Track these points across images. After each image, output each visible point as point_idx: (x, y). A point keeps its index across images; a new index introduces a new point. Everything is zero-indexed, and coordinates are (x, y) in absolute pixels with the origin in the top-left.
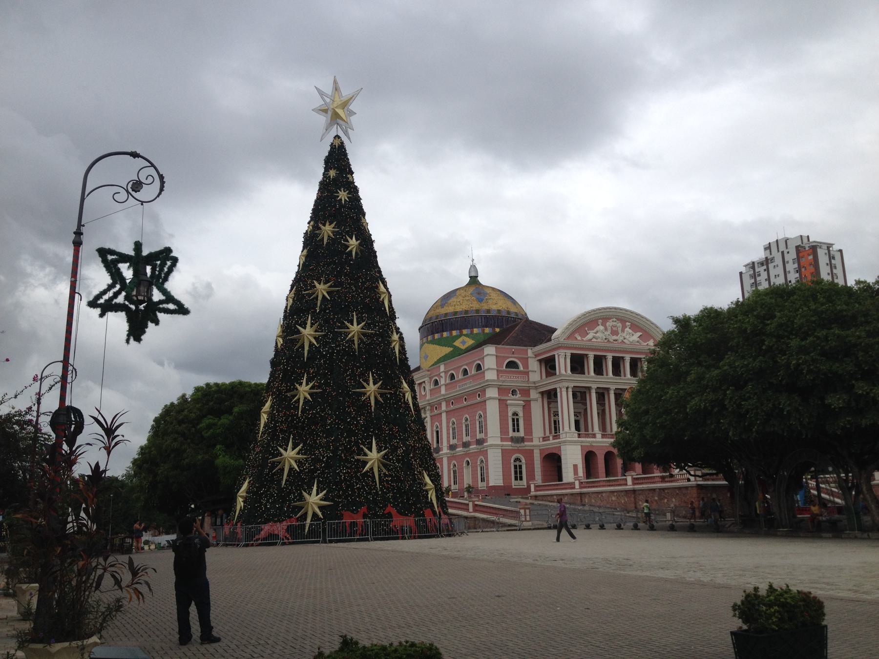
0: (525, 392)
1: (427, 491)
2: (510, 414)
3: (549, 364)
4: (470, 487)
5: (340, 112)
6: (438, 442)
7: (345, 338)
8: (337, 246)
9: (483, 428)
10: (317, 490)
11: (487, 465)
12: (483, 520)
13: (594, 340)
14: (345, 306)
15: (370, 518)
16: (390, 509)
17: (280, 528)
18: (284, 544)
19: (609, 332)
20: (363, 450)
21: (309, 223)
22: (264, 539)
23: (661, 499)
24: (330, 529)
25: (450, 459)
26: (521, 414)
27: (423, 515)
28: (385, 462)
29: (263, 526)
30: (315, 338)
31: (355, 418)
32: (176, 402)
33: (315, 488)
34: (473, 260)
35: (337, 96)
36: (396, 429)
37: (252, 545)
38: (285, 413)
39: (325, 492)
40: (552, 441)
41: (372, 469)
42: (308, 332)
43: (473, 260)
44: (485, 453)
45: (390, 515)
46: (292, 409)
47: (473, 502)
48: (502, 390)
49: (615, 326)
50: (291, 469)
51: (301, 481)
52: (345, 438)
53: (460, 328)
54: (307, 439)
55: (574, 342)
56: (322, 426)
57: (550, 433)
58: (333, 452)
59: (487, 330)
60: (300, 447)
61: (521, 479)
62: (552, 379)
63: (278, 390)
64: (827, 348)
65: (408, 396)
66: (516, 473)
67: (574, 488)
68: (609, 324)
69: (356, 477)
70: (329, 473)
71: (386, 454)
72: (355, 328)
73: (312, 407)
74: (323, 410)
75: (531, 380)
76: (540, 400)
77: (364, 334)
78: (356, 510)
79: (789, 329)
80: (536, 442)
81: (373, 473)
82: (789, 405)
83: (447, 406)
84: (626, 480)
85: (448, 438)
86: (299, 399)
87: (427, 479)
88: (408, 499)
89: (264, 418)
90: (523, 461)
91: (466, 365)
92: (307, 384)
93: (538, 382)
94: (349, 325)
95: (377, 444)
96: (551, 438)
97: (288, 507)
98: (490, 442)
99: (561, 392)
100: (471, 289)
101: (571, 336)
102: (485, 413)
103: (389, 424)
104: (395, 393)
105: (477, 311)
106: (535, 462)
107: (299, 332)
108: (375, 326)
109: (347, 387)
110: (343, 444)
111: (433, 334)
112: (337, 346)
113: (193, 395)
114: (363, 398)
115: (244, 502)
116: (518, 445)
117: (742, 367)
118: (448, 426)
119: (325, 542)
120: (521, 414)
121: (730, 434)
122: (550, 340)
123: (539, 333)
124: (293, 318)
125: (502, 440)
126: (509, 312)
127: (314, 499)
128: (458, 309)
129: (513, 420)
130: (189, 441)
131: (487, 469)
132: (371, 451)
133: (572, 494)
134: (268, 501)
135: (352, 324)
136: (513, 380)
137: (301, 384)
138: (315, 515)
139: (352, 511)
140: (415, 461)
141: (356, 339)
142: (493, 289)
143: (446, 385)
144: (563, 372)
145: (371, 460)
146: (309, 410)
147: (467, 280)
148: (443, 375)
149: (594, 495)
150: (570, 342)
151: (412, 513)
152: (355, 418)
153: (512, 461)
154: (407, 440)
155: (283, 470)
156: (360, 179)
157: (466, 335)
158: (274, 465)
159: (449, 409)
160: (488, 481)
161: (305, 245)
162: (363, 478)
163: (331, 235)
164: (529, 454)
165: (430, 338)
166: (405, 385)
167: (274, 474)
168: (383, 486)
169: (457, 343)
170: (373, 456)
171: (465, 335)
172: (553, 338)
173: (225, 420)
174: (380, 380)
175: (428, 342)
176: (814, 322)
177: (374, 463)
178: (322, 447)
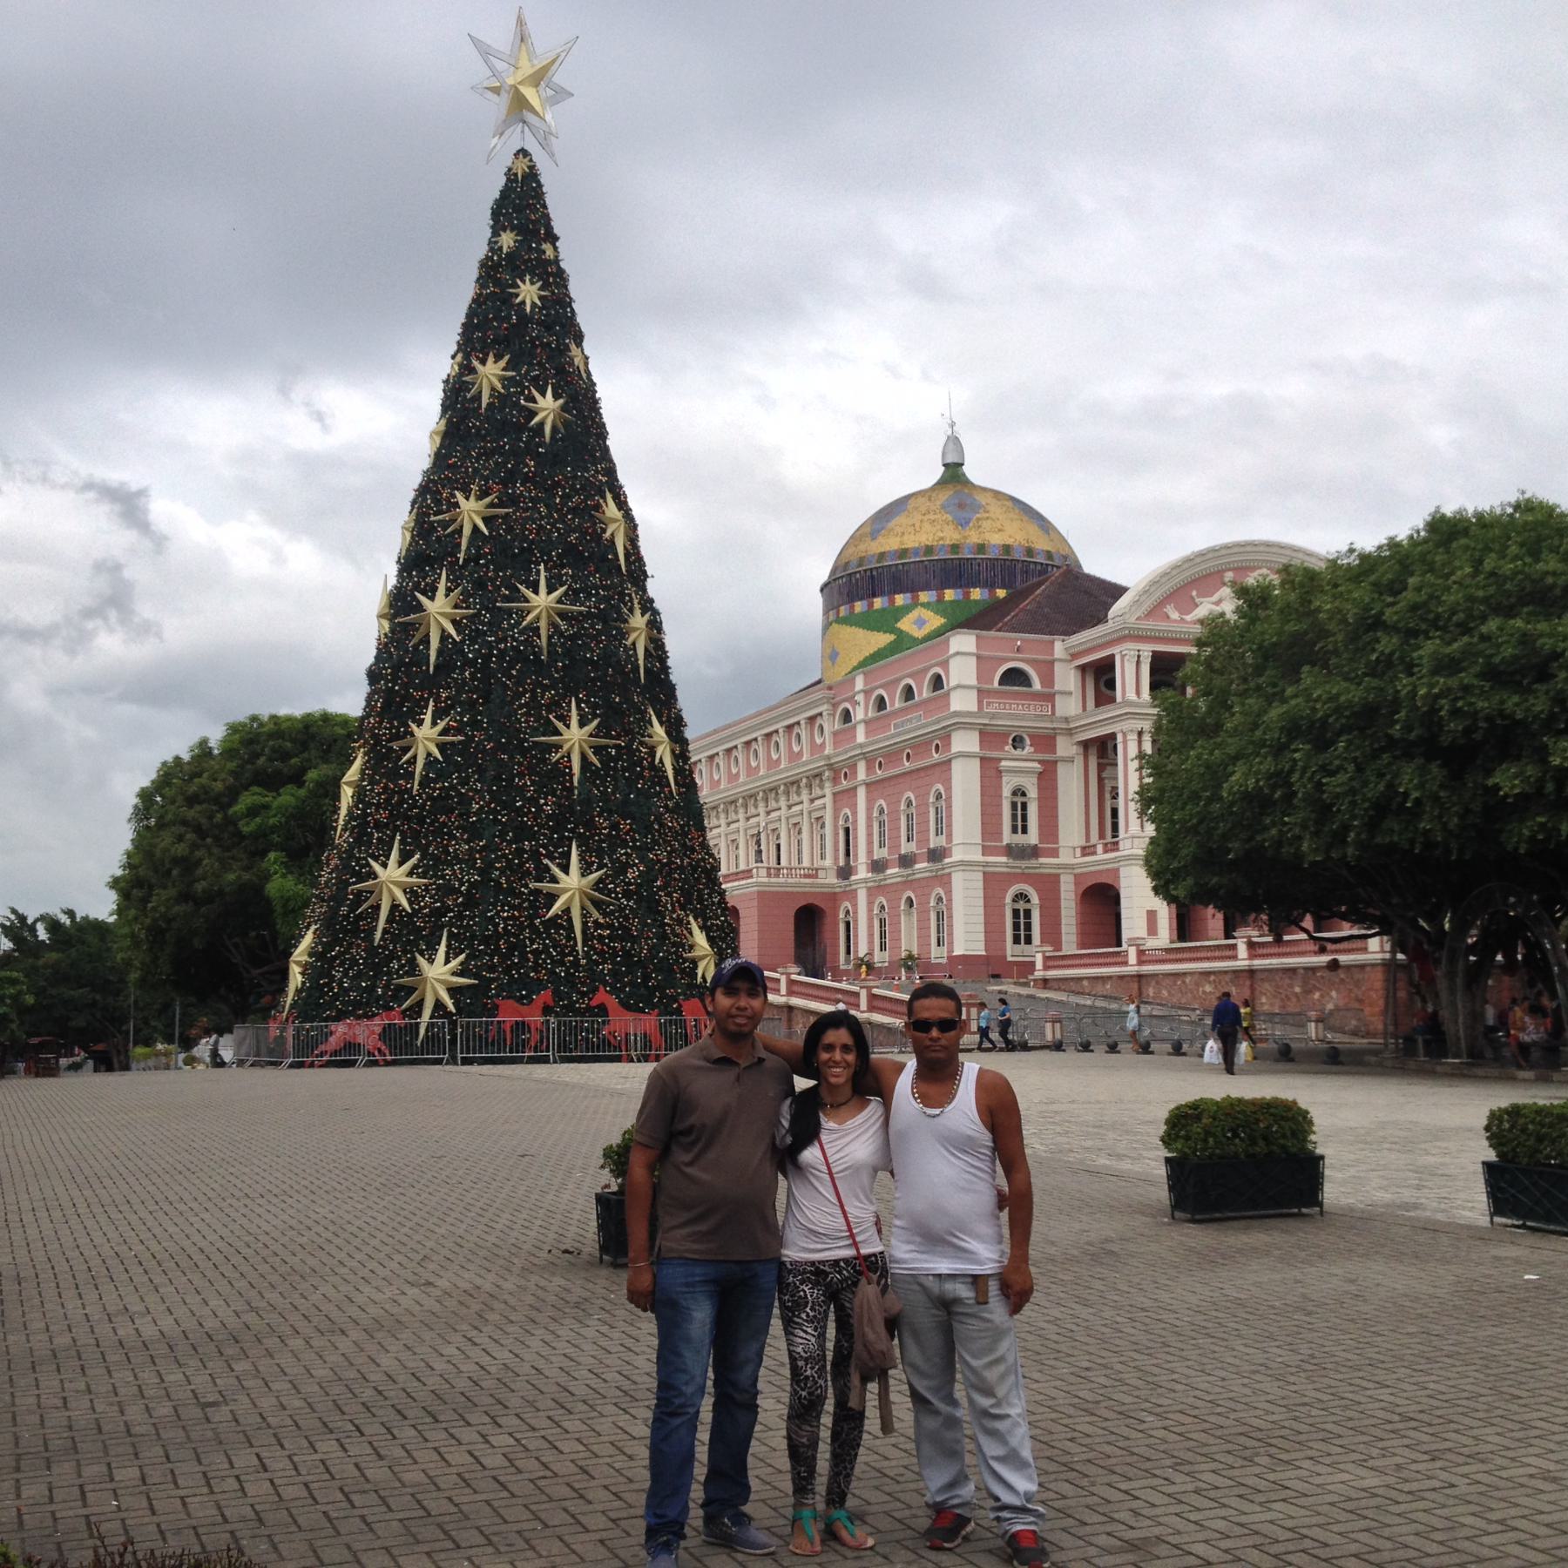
0: (1045, 742)
1: (694, 962)
2: (1006, 792)
3: (1101, 675)
4: (910, 957)
5: (529, 93)
6: (848, 853)
7: (518, 623)
8: (508, 416)
9: (944, 825)
10: (447, 953)
11: (950, 909)
12: (881, 1026)
14: (522, 549)
15: (557, 1015)
16: (603, 996)
17: (366, 1031)
18: (374, 1063)
20: (548, 869)
21: (453, 357)
22: (335, 1053)
23: (1308, 991)
24: (472, 1034)
25: (872, 892)
26: (1033, 793)
27: (679, 1012)
28: (597, 899)
29: (333, 1026)
30: (454, 622)
31: (533, 801)
32: (186, 757)
33: (442, 949)
34: (952, 425)
35: (524, 55)
36: (625, 825)
37: (312, 1065)
38: (385, 788)
39: (462, 957)
40: (1101, 855)
41: (567, 911)
42: (439, 608)
43: (952, 425)
44: (945, 881)
45: (603, 1010)
46: (401, 777)
47: (869, 988)
48: (988, 737)
50: (395, 907)
51: (414, 933)
52: (510, 843)
53: (913, 589)
54: (429, 844)
55: (1162, 625)
56: (461, 815)
57: (1102, 836)
58: (481, 872)
59: (977, 594)
60: (414, 860)
61: (1028, 941)
62: (1108, 712)
63: (374, 736)
64: (1497, 660)
65: (664, 753)
66: (1016, 926)
67: (1126, 963)
69: (532, 926)
70: (472, 918)
71: (600, 880)
72: (542, 601)
73: (442, 775)
74: (464, 782)
75: (1058, 713)
76: (1079, 761)
77: (562, 615)
78: (528, 996)
79: (1431, 616)
80: (1065, 858)
81: (570, 920)
82: (1421, 786)
83: (869, 769)
84: (1234, 947)
85: (870, 843)
86: (415, 757)
87: (700, 938)
88: (646, 978)
89: (347, 793)
90: (1035, 900)
91: (909, 676)
92: (434, 724)
93: (1078, 718)
94: (529, 593)
95: (582, 858)
96: (1100, 848)
97: (386, 987)
98: (957, 855)
99: (1125, 742)
100: (944, 496)
101: (1156, 611)
102: (949, 789)
103: (610, 812)
104: (629, 746)
105: (955, 548)
106: (1063, 904)
107: (420, 608)
108: (589, 596)
109: (519, 731)
110: (505, 856)
111: (851, 598)
112: (499, 641)
113: (224, 741)
114: (555, 757)
115: (303, 974)
116: (1024, 864)
117: (1330, 699)
118: (869, 818)
119: (455, 1063)
120: (1033, 793)
121: (1305, 846)
122: (1101, 619)
123: (1085, 599)
124: (410, 576)
125: (986, 851)
126: (1030, 552)
127: (439, 972)
128: (911, 542)
129: (1014, 805)
130: (209, 840)
131: (950, 917)
132: (566, 872)
133: (1121, 977)
134: (345, 974)
135: (536, 592)
136: (1016, 713)
137: (420, 723)
138: (439, 1005)
139: (520, 999)
140: (669, 895)
141: (543, 624)
142: (997, 494)
143: (867, 722)
144: (1131, 696)
145: (565, 890)
146: (435, 781)
147: (940, 471)
148: (860, 698)
149: (1168, 981)
150: (1150, 624)
151: (653, 1007)
152: (533, 801)
153: (1008, 899)
154: (651, 850)
155: (377, 908)
156: (572, 254)
157: (926, 605)
158: (360, 897)
159: (873, 778)
160: (951, 943)
161: (445, 408)
162: (547, 931)
163: (499, 386)
164: (1049, 885)
165: (843, 611)
166: (659, 730)
167: (360, 917)
168: (592, 947)
169: (906, 624)
170: (572, 884)
171: (923, 605)
172: (1111, 613)
173: (287, 797)
174: (595, 716)
175: (839, 621)
176: (1485, 600)
177: (571, 899)
178: (460, 862)
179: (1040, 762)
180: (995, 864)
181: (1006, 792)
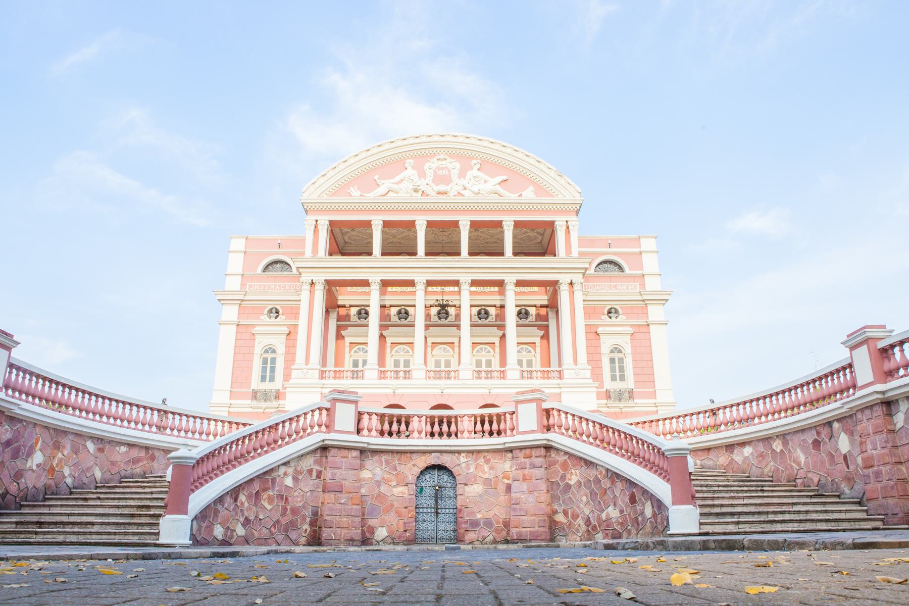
2: (258, 349)
13: (391, 194)
19: (429, 179)
49: (443, 169)
68: (431, 166)
116: (263, 404)
120: (281, 349)
125: (233, 395)
129: (265, 361)
179: (288, 326)
181: (258, 349)
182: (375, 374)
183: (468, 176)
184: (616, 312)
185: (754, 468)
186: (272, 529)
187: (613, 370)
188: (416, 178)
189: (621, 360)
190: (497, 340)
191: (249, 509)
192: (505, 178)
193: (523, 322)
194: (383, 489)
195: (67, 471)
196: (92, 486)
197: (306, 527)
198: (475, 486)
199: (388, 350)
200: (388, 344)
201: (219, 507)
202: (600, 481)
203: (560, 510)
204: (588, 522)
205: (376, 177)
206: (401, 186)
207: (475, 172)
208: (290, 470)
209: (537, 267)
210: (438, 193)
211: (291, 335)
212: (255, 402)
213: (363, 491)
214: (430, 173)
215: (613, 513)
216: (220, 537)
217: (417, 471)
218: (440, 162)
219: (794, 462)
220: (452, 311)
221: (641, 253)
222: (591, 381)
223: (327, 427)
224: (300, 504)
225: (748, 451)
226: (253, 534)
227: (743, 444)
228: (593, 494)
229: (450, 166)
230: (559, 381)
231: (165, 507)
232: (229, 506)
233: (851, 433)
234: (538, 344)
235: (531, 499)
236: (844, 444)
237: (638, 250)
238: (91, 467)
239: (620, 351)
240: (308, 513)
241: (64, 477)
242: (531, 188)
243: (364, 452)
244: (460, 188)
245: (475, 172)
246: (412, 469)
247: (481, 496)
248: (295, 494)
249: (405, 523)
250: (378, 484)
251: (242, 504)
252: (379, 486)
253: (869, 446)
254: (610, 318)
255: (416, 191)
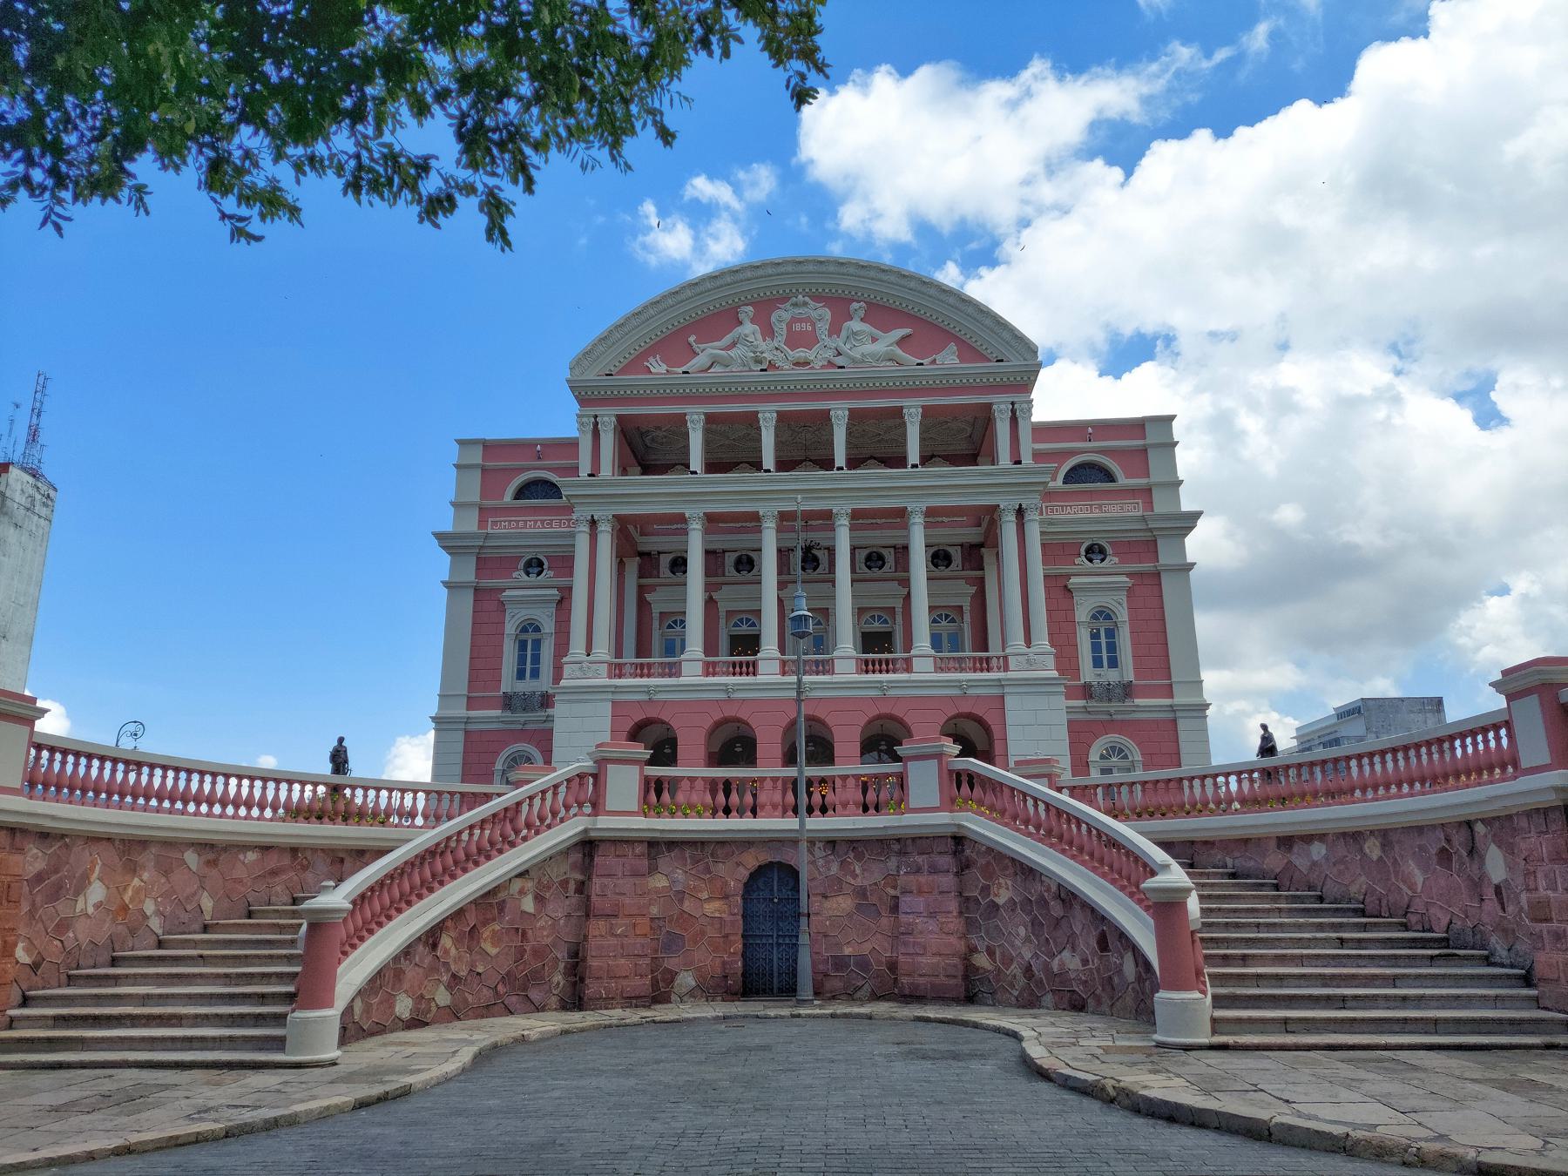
2: (510, 628)
13: (717, 369)
19: (780, 340)
116: (522, 717)
120: (548, 626)
125: (471, 703)
129: (523, 646)
179: (559, 589)
180: (489, 720)
181: (510, 628)
182: (699, 668)
183: (844, 334)
184: (1102, 551)
185: (1329, 881)
186: (500, 987)
187: (1096, 648)
188: (759, 336)
189: (1111, 633)
190: (898, 604)
191: (459, 959)
192: (907, 331)
193: (943, 571)
194: (687, 905)
195: (149, 907)
196: (196, 926)
197: (558, 978)
198: (840, 899)
199: (722, 622)
200: (722, 614)
201: (404, 964)
202: (1046, 903)
203: (981, 946)
204: (1028, 970)
205: (692, 339)
206: (732, 353)
207: (856, 325)
208: (530, 885)
209: (960, 486)
210: (797, 364)
211: (564, 601)
212: (509, 714)
213: (654, 910)
214: (781, 329)
215: (1069, 961)
216: (406, 1015)
217: (744, 874)
218: (797, 311)
219: (1404, 882)
220: (821, 555)
221: (1144, 451)
222: (1055, 674)
223: (594, 805)
224: (549, 941)
225: (1318, 851)
226: (466, 1000)
227: (1308, 839)
228: (1035, 924)
229: (814, 314)
230: (1001, 675)
231: (290, 998)
232: (421, 960)
233: (1509, 849)
234: (967, 609)
235: (932, 925)
236: (1496, 866)
237: (1140, 442)
238: (195, 894)
239: (1108, 617)
240: (561, 954)
241: (146, 917)
242: (953, 347)
243: (656, 846)
244: (829, 354)
245: (856, 325)
246: (735, 874)
247: (850, 915)
248: (541, 923)
249: (724, 963)
250: (681, 896)
251: (446, 952)
252: (681, 901)
253: (1542, 883)
254: (1091, 561)
255: (758, 361)
